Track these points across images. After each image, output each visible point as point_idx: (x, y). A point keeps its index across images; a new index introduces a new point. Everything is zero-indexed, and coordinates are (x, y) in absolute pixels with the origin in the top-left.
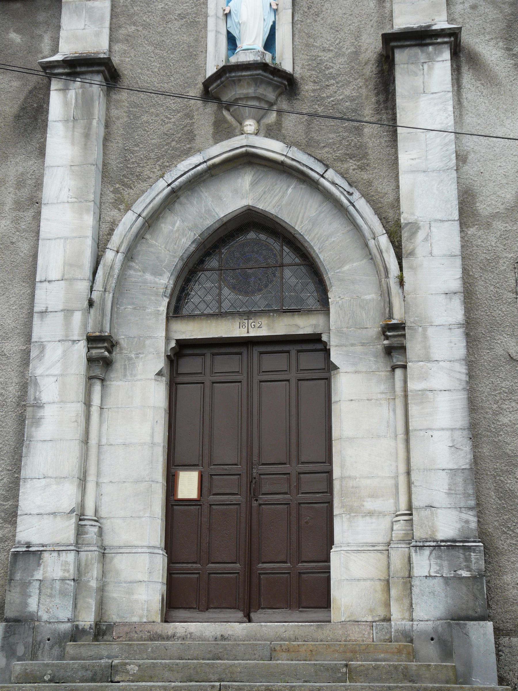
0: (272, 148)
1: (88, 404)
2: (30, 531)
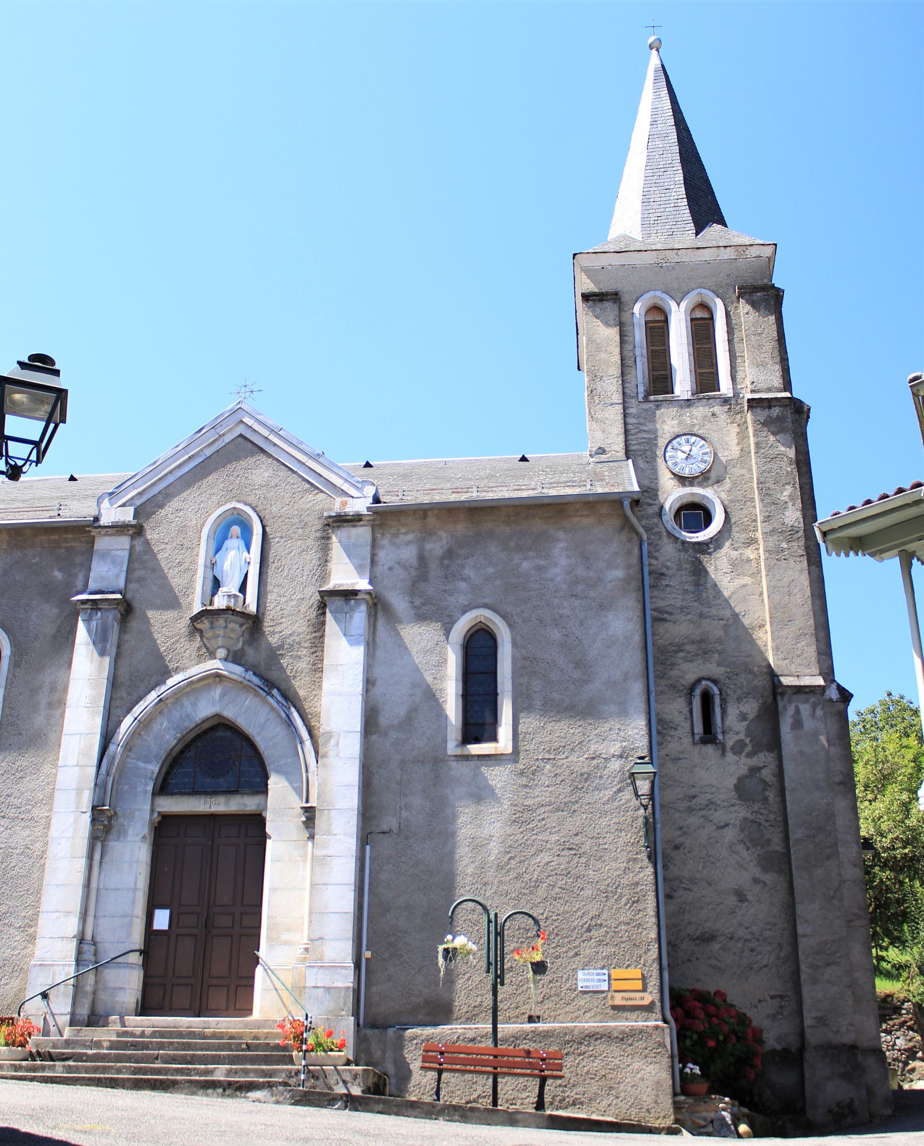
1: (90, 857)
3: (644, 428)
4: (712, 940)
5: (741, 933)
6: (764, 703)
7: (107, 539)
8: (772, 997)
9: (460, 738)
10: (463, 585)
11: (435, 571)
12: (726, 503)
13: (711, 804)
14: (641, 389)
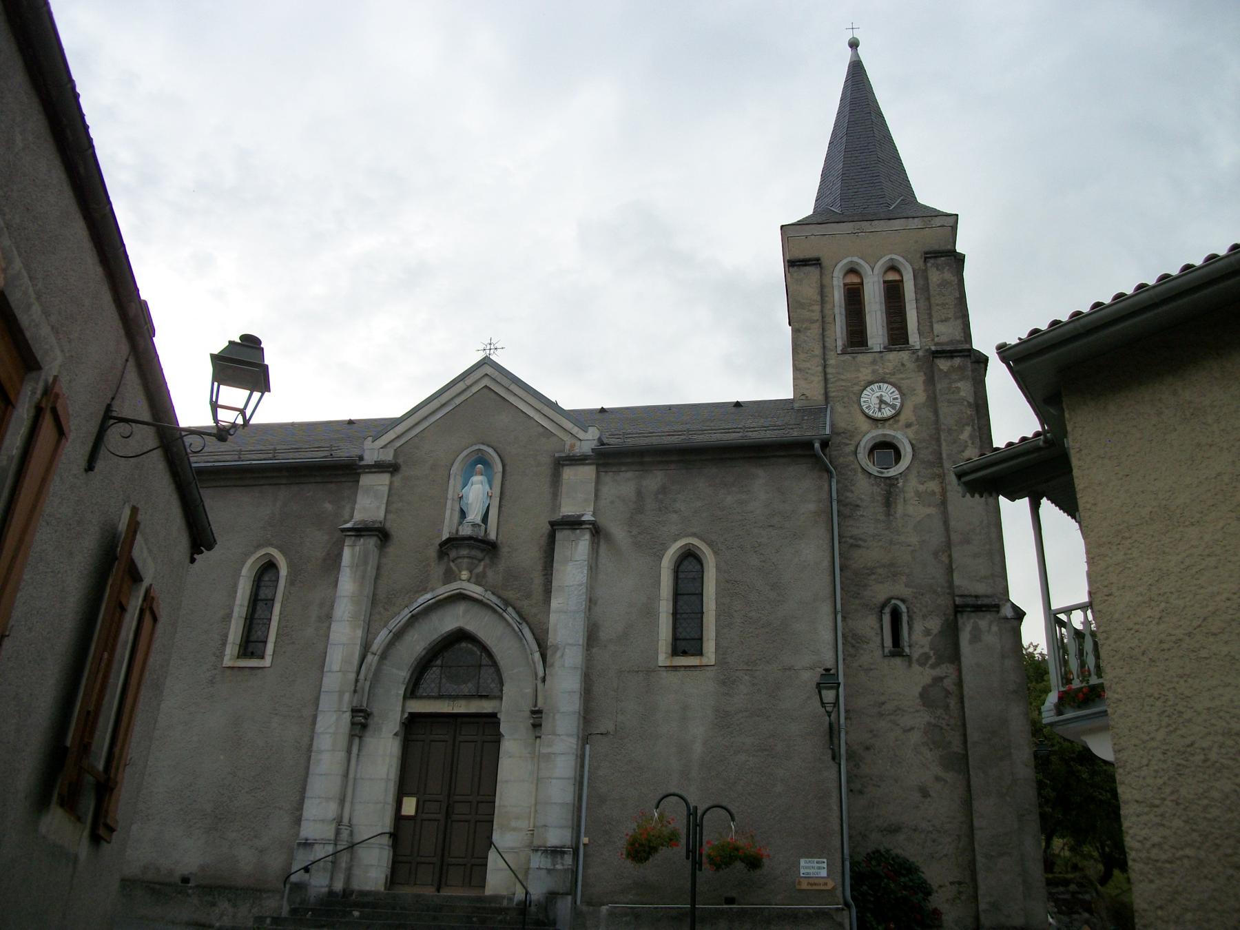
0: (475, 590)
1: (349, 752)
2: (309, 830)
7: (371, 476)
10: (674, 517)
14: (840, 343)
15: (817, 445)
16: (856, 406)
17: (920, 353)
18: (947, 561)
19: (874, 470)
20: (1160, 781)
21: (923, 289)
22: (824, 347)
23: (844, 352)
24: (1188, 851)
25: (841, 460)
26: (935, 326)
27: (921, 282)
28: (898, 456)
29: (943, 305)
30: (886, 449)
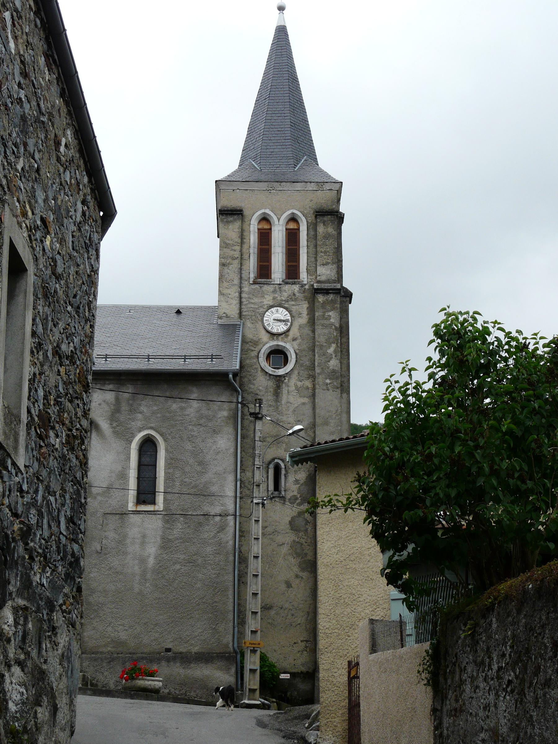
3: (253, 301)
4: (271, 609)
5: (287, 605)
6: (309, 475)
8: (302, 641)
9: (135, 501)
10: (140, 416)
11: (124, 407)
12: (297, 351)
13: (275, 532)
14: (252, 276)
15: (231, 376)
16: (260, 323)
17: (307, 287)
18: (313, 436)
19: (270, 370)
20: (331, 608)
21: (313, 237)
22: (241, 278)
23: (255, 283)
24: (336, 631)
25: (248, 361)
26: (318, 268)
27: (312, 233)
28: (286, 361)
29: (325, 252)
30: (278, 355)
